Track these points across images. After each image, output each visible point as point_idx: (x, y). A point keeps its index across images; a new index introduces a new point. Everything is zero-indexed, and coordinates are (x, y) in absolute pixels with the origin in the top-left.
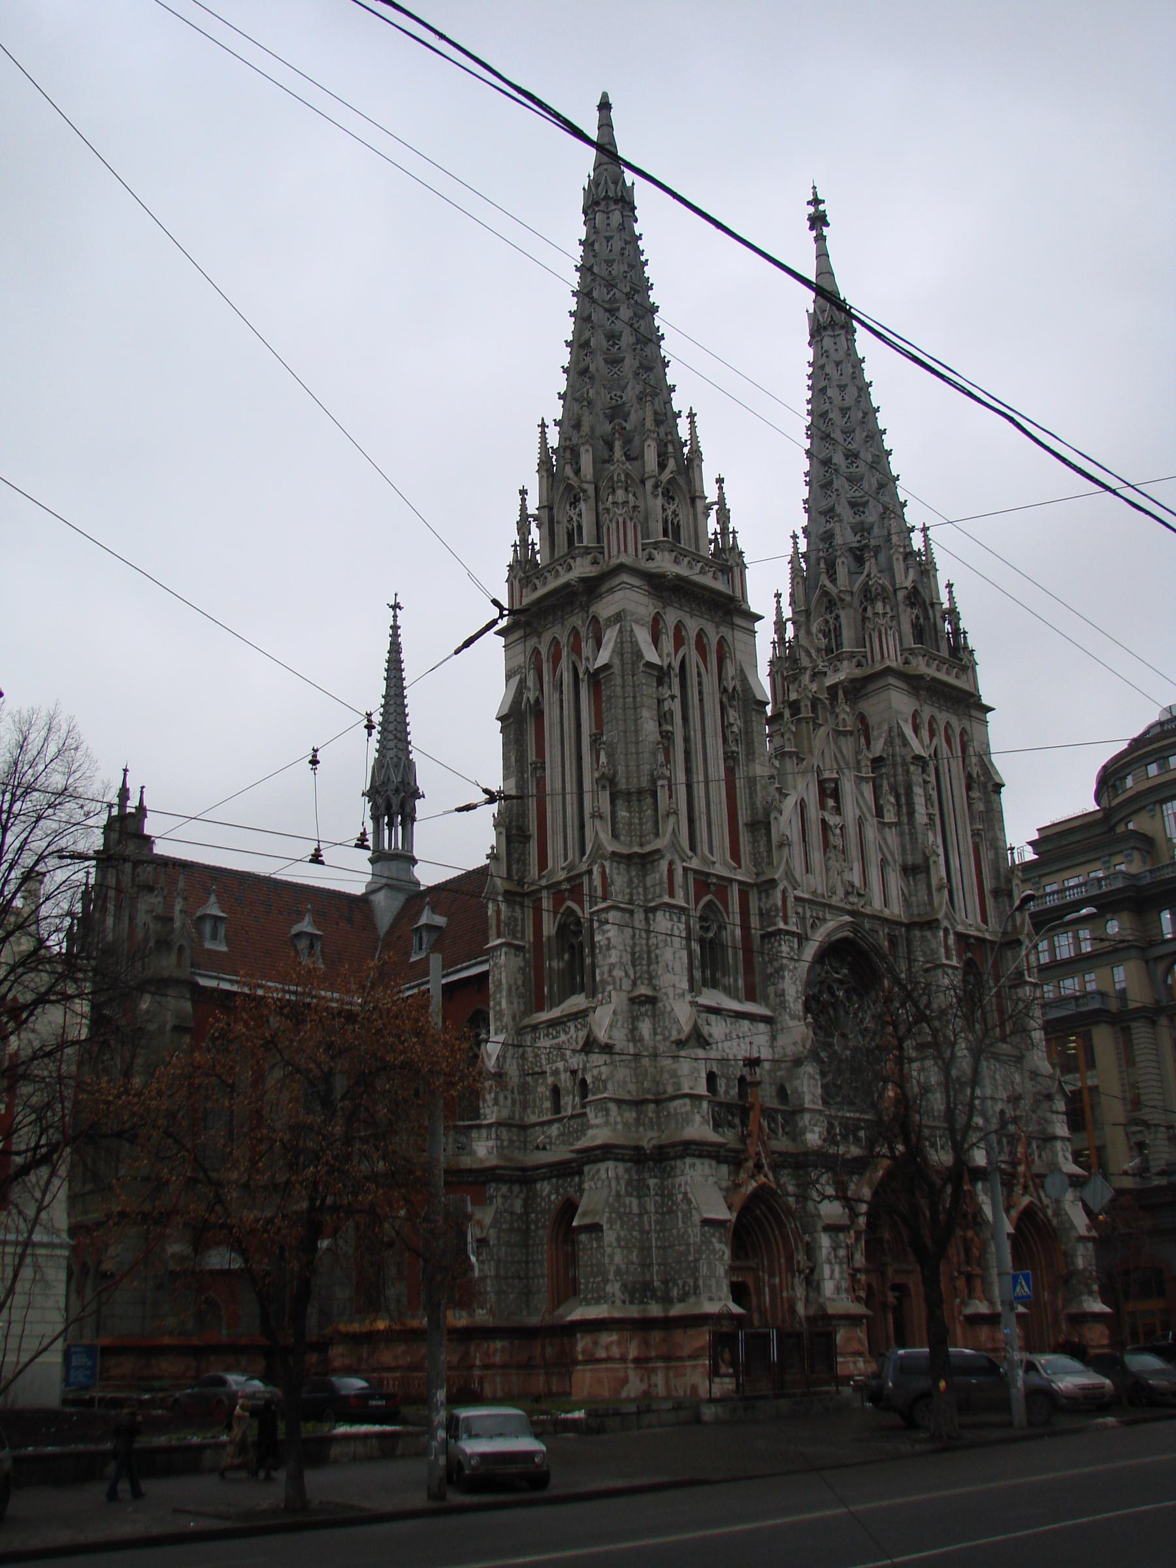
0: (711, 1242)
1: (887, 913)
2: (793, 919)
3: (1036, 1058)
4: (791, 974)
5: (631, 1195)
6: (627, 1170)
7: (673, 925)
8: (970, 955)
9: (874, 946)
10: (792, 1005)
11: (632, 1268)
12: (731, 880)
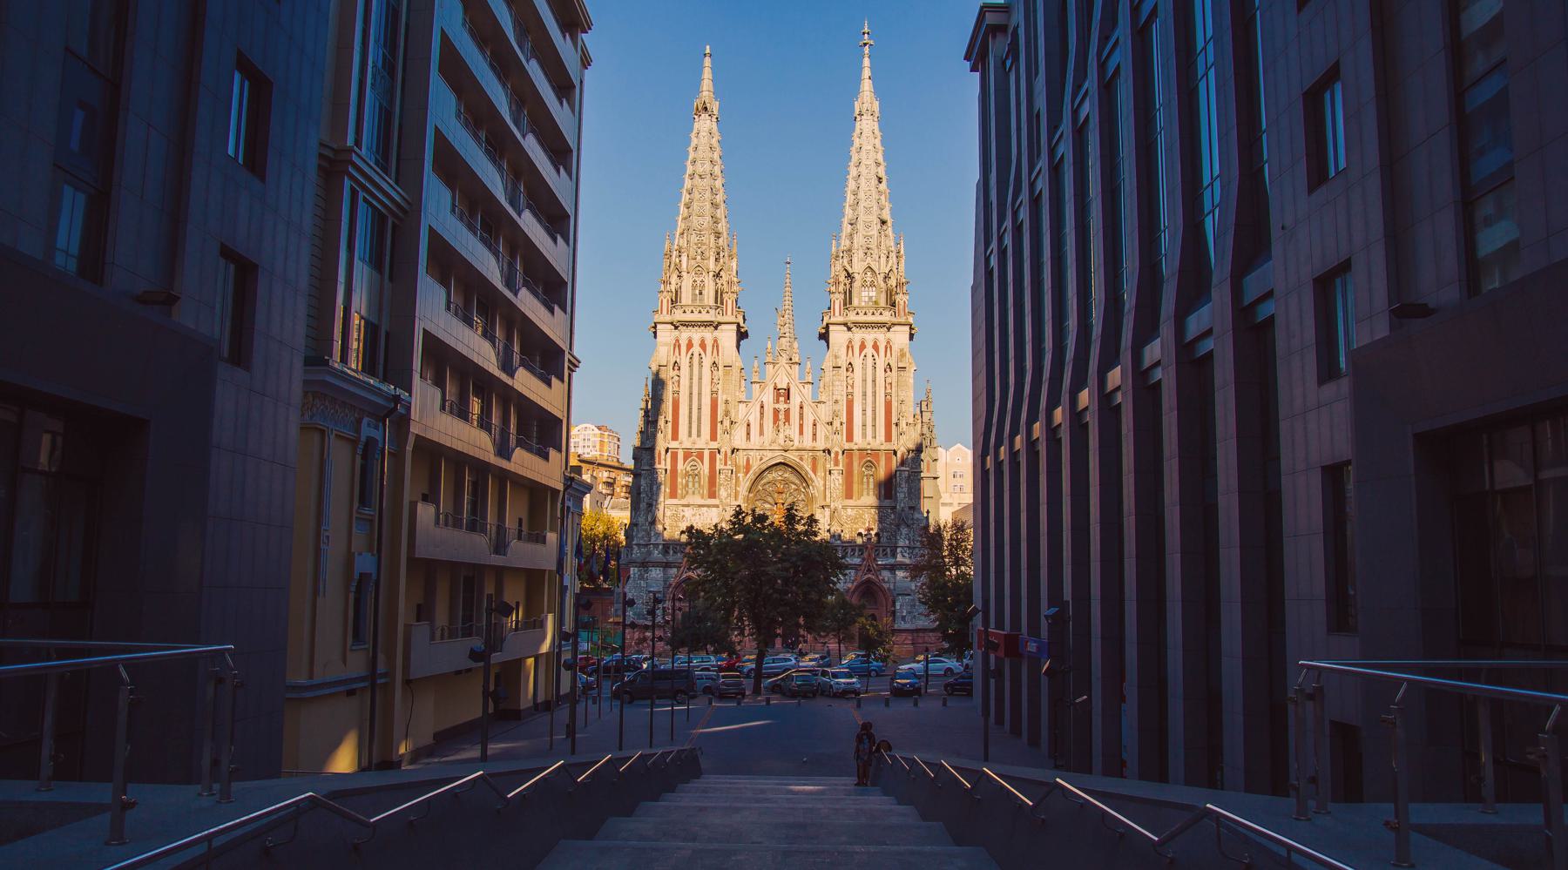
2: (729, 463)
6: (639, 571)
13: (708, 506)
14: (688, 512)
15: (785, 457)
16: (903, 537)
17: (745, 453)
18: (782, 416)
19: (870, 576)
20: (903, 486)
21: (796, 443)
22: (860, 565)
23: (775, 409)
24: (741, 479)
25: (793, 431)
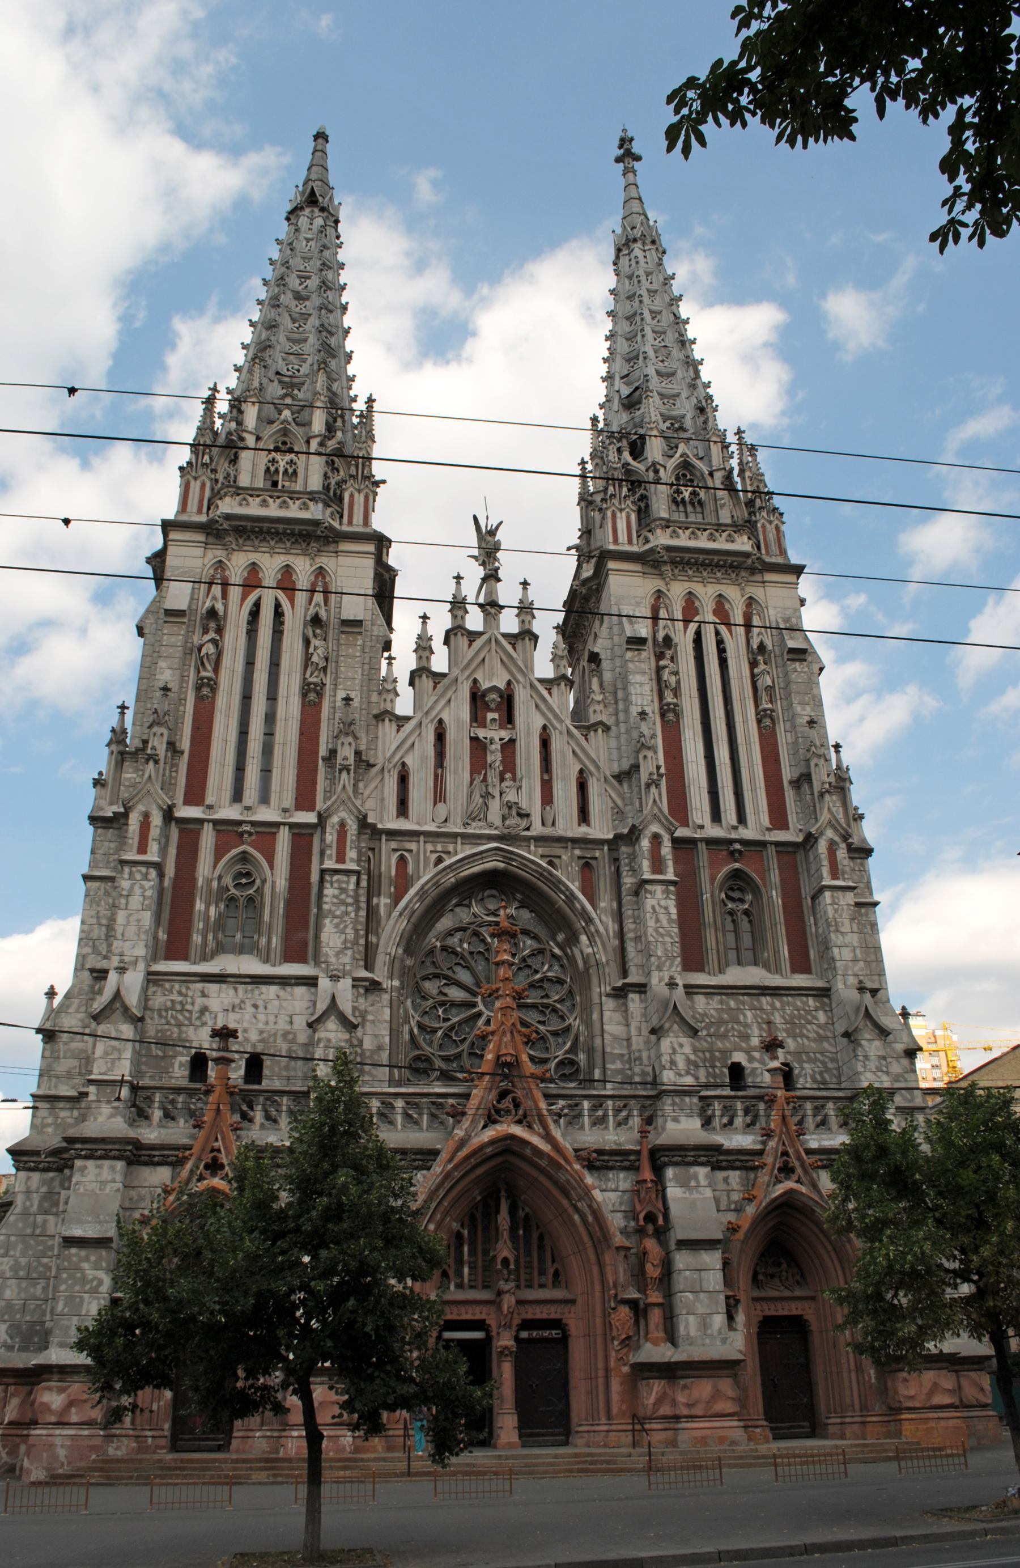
0: (81, 1270)
1: (582, 831)
2: (352, 854)
3: (840, 986)
4: (336, 921)
5: (46, 1213)
6: (43, 1182)
7: (132, 886)
8: (737, 865)
9: (541, 875)
10: (333, 960)
11: (32, 1305)
12: (277, 825)
13: (283, 981)
14: (219, 997)
15: (508, 857)
16: (872, 1065)
17: (393, 845)
18: (494, 757)
19: (790, 1184)
20: (846, 927)
21: (537, 829)
22: (760, 1153)
23: (475, 740)
24: (382, 910)
25: (530, 798)
